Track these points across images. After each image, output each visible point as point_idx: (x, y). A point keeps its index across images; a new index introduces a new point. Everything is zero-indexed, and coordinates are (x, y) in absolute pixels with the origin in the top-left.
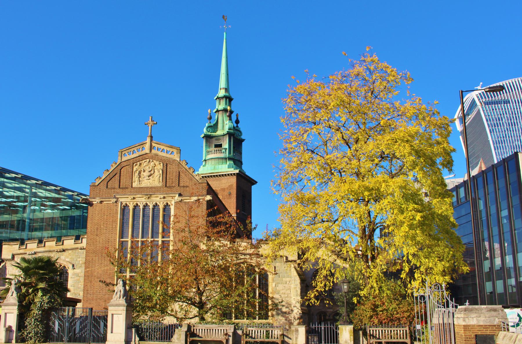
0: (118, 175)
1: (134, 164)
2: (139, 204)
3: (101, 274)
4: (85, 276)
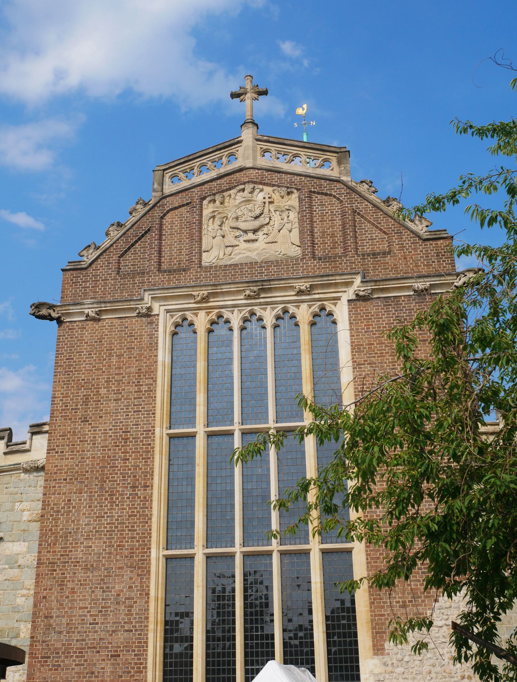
0: (154, 234)
1: (205, 202)
2: (227, 314)
3: (100, 554)
4: (40, 563)
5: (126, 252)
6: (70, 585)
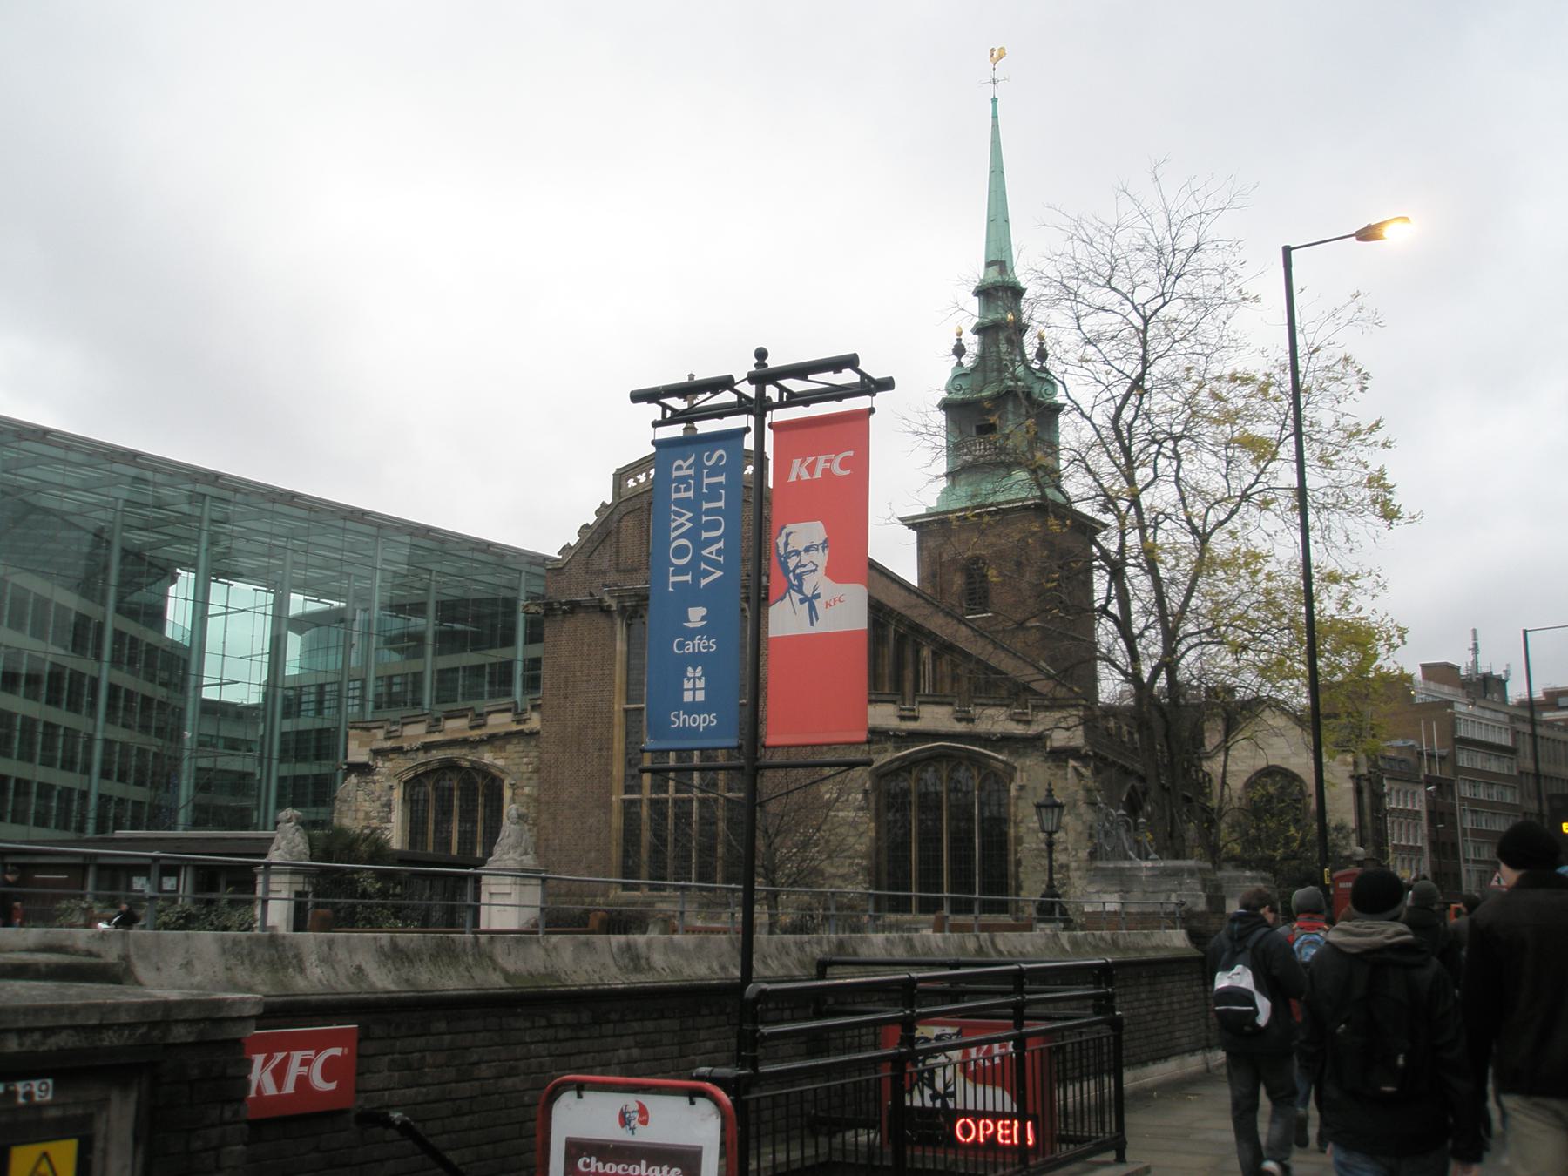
5: (592, 553)
6: (560, 819)
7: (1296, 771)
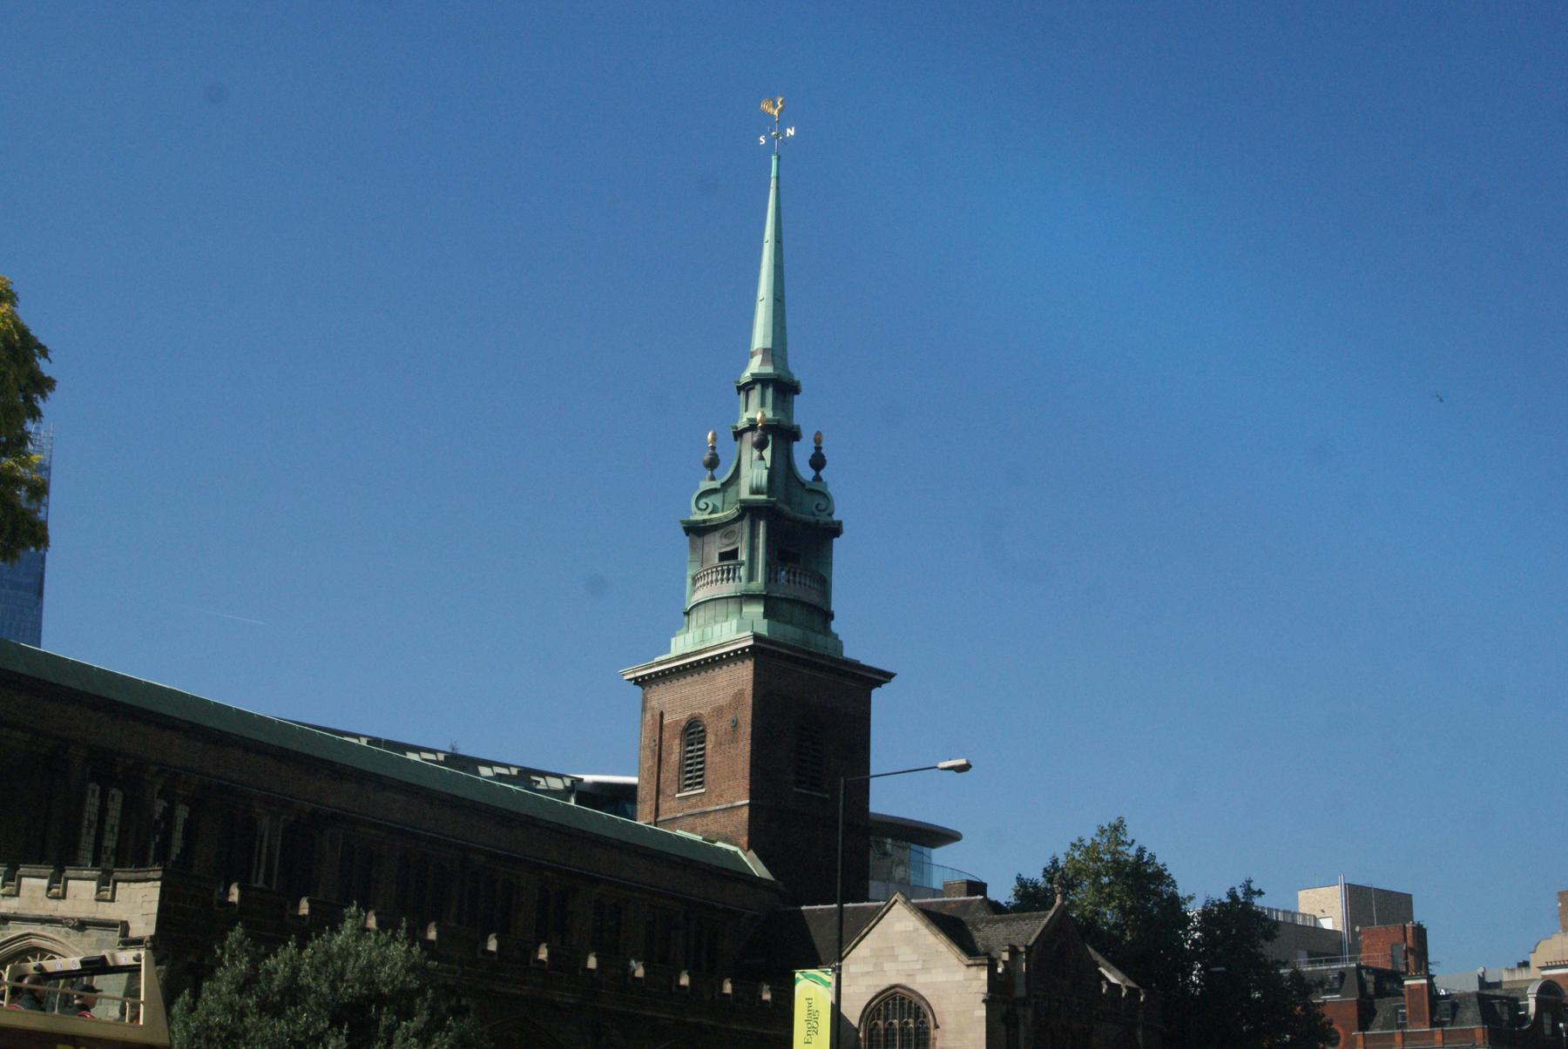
7: (923, 993)
